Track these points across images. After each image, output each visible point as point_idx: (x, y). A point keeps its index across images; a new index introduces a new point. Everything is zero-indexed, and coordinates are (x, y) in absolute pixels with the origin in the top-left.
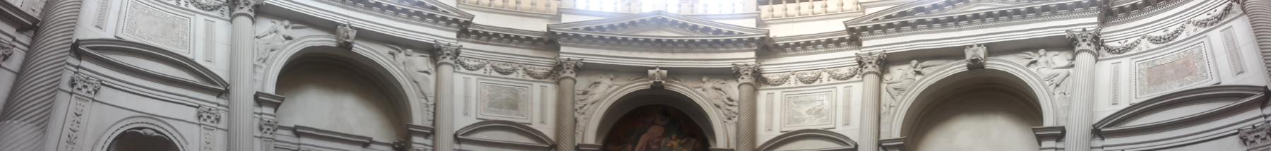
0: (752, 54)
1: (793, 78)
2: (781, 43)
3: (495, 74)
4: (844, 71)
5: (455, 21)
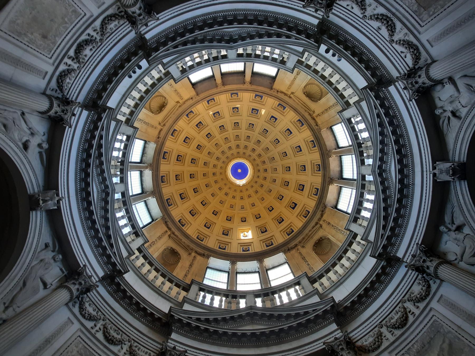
0: (334, 326)
1: (384, 330)
2: (348, 303)
3: (100, 336)
4: (417, 289)
5: (114, 265)
